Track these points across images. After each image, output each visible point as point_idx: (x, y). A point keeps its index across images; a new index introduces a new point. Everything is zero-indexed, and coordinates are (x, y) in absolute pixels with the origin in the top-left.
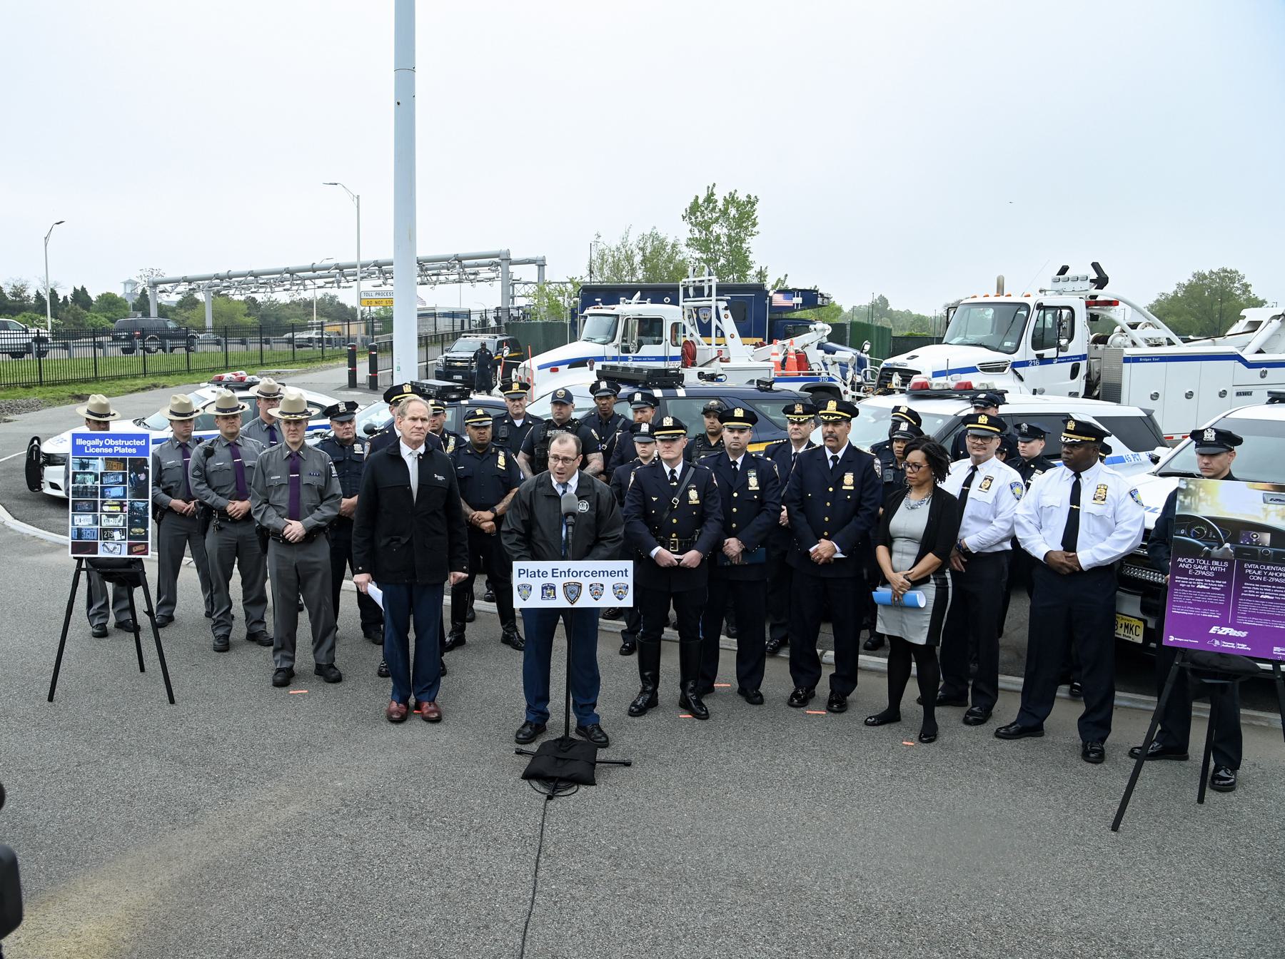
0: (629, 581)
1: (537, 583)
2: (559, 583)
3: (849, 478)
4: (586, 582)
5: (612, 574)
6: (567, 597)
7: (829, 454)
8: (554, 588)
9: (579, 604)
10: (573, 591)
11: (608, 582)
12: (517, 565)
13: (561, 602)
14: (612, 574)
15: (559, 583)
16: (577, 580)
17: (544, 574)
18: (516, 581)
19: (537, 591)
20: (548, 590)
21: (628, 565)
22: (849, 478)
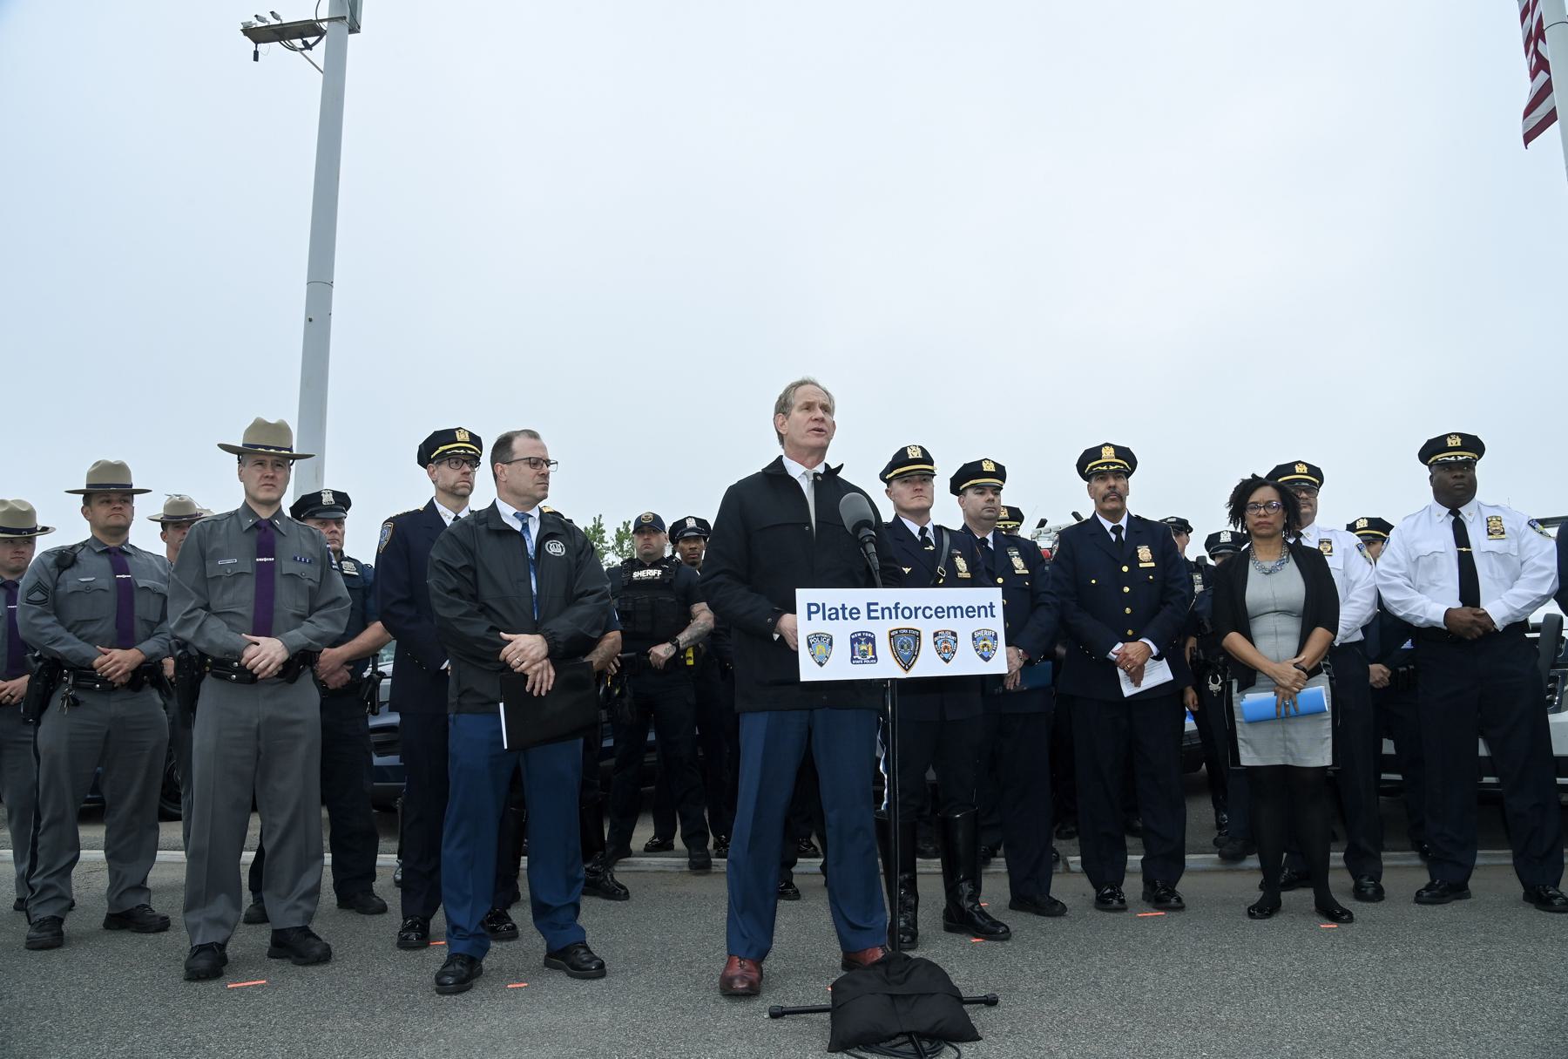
0: (997, 624)
1: (842, 632)
2: (881, 630)
3: (1144, 553)
4: (927, 627)
5: (969, 612)
6: (897, 656)
7: (1108, 525)
8: (871, 640)
9: (918, 671)
10: (906, 644)
11: (965, 628)
12: (804, 596)
13: (886, 668)
14: (969, 612)
15: (881, 630)
16: (911, 623)
17: (854, 613)
19: (842, 648)
20: (862, 644)
22: (1144, 553)
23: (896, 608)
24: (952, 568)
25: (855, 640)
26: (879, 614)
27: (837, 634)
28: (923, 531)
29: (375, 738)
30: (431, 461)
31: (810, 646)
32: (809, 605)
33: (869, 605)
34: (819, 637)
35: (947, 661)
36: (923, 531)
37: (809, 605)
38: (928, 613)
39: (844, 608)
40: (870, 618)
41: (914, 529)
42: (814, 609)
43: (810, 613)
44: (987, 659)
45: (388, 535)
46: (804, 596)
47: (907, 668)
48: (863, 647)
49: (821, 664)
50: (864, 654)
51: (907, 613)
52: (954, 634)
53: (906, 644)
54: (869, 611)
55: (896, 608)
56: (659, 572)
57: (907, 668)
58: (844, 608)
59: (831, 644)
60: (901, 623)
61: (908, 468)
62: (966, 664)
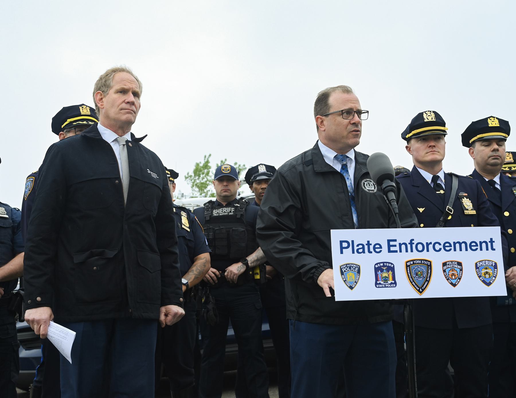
0: (497, 256)
1: (367, 262)
2: (399, 261)
4: (437, 259)
5: (473, 246)
8: (391, 269)
9: (429, 293)
10: (420, 273)
11: (469, 259)
12: (337, 236)
13: (404, 290)
14: (473, 246)
15: (399, 261)
16: (424, 256)
17: (377, 248)
19: (368, 275)
20: (384, 272)
23: (411, 243)
24: (459, 207)
25: (378, 269)
26: (397, 248)
27: (362, 267)
28: (435, 178)
29: (21, 336)
30: (63, 130)
31: (342, 273)
32: (341, 242)
33: (389, 241)
34: (349, 266)
35: (454, 285)
36: (435, 178)
37: (341, 242)
38: (437, 247)
39: (369, 244)
40: (390, 251)
41: (428, 177)
42: (345, 245)
43: (342, 248)
44: (489, 284)
45: (31, 185)
46: (337, 236)
47: (421, 290)
48: (385, 274)
49: (351, 288)
50: (386, 279)
51: (420, 247)
52: (460, 264)
53: (420, 273)
54: (389, 246)
55: (411, 243)
56: (233, 209)
57: (421, 290)
58: (369, 244)
59: (359, 272)
60: (416, 255)
61: (425, 130)
62: (471, 287)
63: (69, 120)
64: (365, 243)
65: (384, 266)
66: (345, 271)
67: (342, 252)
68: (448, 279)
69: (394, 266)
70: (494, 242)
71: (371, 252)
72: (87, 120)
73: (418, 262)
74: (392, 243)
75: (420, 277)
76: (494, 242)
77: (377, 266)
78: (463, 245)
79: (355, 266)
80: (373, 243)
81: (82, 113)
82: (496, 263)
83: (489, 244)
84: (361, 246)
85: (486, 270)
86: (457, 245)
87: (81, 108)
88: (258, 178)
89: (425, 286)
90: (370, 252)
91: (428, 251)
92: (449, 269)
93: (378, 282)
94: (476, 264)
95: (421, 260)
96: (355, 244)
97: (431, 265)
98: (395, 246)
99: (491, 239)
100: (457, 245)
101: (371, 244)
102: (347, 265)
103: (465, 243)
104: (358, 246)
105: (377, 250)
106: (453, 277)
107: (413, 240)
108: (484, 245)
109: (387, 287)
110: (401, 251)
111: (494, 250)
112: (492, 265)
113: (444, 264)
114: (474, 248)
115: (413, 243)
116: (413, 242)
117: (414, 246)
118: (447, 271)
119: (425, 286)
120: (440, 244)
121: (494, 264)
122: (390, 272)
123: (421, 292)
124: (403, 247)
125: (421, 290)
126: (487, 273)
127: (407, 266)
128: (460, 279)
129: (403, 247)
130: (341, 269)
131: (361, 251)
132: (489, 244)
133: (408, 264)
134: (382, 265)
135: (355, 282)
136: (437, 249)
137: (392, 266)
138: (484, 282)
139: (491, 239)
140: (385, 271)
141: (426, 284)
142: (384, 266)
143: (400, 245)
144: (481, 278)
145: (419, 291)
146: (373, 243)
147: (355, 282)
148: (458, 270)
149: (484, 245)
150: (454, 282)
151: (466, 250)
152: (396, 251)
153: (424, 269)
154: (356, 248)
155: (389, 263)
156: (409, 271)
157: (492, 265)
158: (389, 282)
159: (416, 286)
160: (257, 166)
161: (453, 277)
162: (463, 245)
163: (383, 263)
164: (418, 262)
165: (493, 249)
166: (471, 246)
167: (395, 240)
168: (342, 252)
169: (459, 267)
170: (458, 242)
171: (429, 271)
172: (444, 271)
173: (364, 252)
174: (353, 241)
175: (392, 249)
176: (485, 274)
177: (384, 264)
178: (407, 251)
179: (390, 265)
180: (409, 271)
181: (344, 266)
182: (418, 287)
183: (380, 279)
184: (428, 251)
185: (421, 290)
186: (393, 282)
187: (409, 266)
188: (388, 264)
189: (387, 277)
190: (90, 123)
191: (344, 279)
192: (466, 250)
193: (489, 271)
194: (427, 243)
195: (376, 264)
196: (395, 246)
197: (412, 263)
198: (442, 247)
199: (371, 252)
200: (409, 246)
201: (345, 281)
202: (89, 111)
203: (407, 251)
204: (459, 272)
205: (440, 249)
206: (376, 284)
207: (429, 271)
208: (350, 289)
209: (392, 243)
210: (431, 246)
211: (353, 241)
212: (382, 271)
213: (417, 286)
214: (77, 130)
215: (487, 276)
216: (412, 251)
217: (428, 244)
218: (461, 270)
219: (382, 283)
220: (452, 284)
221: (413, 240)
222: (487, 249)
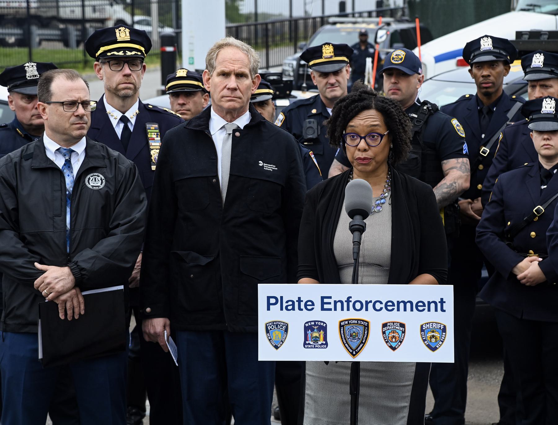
0: (447, 318)
1: (296, 321)
2: (332, 320)
4: (376, 320)
5: (419, 306)
8: (323, 328)
10: (355, 334)
11: (413, 321)
12: (265, 290)
14: (419, 306)
15: (332, 320)
16: (362, 315)
17: (309, 305)
18: (264, 316)
19: (296, 334)
20: (315, 332)
21: (447, 292)
23: (348, 301)
25: (308, 328)
26: (332, 306)
31: (267, 331)
32: (269, 298)
33: (323, 298)
34: (276, 324)
35: (394, 349)
37: (269, 298)
38: (378, 306)
39: (299, 300)
40: (323, 309)
42: (272, 301)
43: (269, 304)
44: (434, 349)
46: (265, 290)
47: (354, 352)
48: (315, 334)
49: (277, 347)
50: (316, 340)
51: (358, 306)
52: (402, 325)
54: (323, 303)
55: (348, 301)
57: (354, 352)
58: (299, 300)
59: (286, 330)
60: (352, 315)
63: (102, 49)
64: (295, 299)
65: (315, 325)
66: (271, 329)
67: (268, 309)
68: (387, 342)
69: (326, 326)
70: (445, 302)
71: (302, 310)
72: (124, 49)
73: (354, 322)
74: (326, 300)
75: (354, 339)
76: (445, 302)
77: (307, 325)
78: (408, 305)
79: (282, 324)
80: (304, 300)
81: (119, 39)
82: (445, 327)
83: (439, 305)
84: (290, 303)
85: (432, 334)
86: (402, 305)
87: (117, 31)
88: (476, 60)
89: (359, 348)
90: (300, 309)
91: (367, 310)
92: (390, 331)
93: (307, 342)
94: (422, 326)
95: (358, 320)
96: (284, 301)
97: (368, 326)
98: (330, 303)
99: (442, 299)
100: (402, 305)
101: (302, 301)
102: (273, 322)
103: (411, 303)
104: (287, 302)
105: (309, 307)
106: (394, 340)
107: (351, 297)
108: (433, 305)
109: (317, 348)
110: (335, 309)
111: (445, 311)
112: (440, 328)
113: (385, 325)
114: (420, 308)
115: (351, 301)
116: (350, 299)
117: (351, 304)
118: (387, 332)
119: (359, 348)
120: (381, 303)
121: (442, 327)
122: (322, 332)
123: (354, 355)
124: (339, 305)
125: (354, 353)
126: (433, 336)
127: (341, 326)
128: (401, 342)
129: (339, 305)
130: (267, 327)
131: (290, 308)
132: (439, 305)
133: (342, 324)
134: (313, 323)
135: (282, 341)
136: (378, 308)
137: (324, 325)
138: (428, 346)
139: (442, 299)
140: (315, 330)
141: (360, 347)
142: (315, 325)
143: (335, 302)
144: (426, 342)
145: (352, 353)
146: (304, 300)
147: (282, 341)
148: (400, 333)
149: (433, 305)
150: (394, 345)
151: (412, 310)
152: (330, 310)
153: (360, 329)
154: (285, 305)
155: (321, 322)
156: (342, 332)
157: (440, 328)
158: (320, 343)
159: (349, 348)
160: (479, 40)
161: (394, 340)
162: (408, 305)
163: (315, 321)
164: (354, 322)
165: (443, 310)
166: (417, 306)
167: (330, 298)
168: (268, 309)
169: (401, 329)
170: (403, 302)
171: (366, 333)
172: (384, 333)
173: (293, 309)
174: (282, 298)
175: (326, 306)
176: (431, 338)
177: (315, 323)
178: (342, 309)
179: (322, 324)
180: (342, 332)
181: (270, 324)
182: (352, 350)
183: (309, 339)
184: (367, 310)
185: (354, 353)
186: (324, 342)
187: (343, 326)
188: (319, 323)
189: (317, 337)
190: (129, 53)
191: (270, 338)
192: (412, 310)
193: (436, 334)
194: (366, 302)
195: (306, 323)
196: (330, 303)
197: (347, 322)
198: (383, 306)
199: (302, 310)
200: (345, 304)
201: (270, 340)
202: (128, 34)
203: (342, 309)
204: (400, 335)
205: (381, 309)
206: (305, 344)
207: (366, 333)
208: (274, 349)
209: (326, 300)
210: (370, 306)
211: (282, 298)
212: (313, 330)
213: (351, 348)
214: (112, 62)
215: (433, 340)
216: (348, 309)
217: (367, 303)
218: (404, 332)
219: (311, 343)
220: (391, 347)
221: (351, 297)
222: (436, 310)
